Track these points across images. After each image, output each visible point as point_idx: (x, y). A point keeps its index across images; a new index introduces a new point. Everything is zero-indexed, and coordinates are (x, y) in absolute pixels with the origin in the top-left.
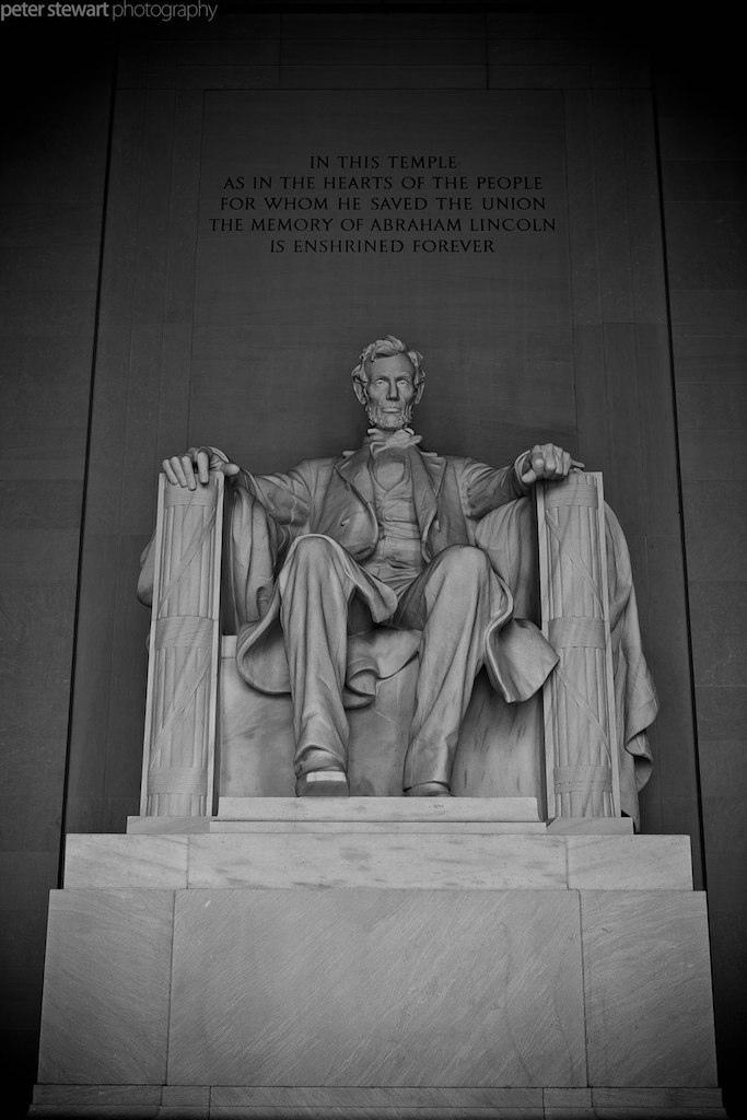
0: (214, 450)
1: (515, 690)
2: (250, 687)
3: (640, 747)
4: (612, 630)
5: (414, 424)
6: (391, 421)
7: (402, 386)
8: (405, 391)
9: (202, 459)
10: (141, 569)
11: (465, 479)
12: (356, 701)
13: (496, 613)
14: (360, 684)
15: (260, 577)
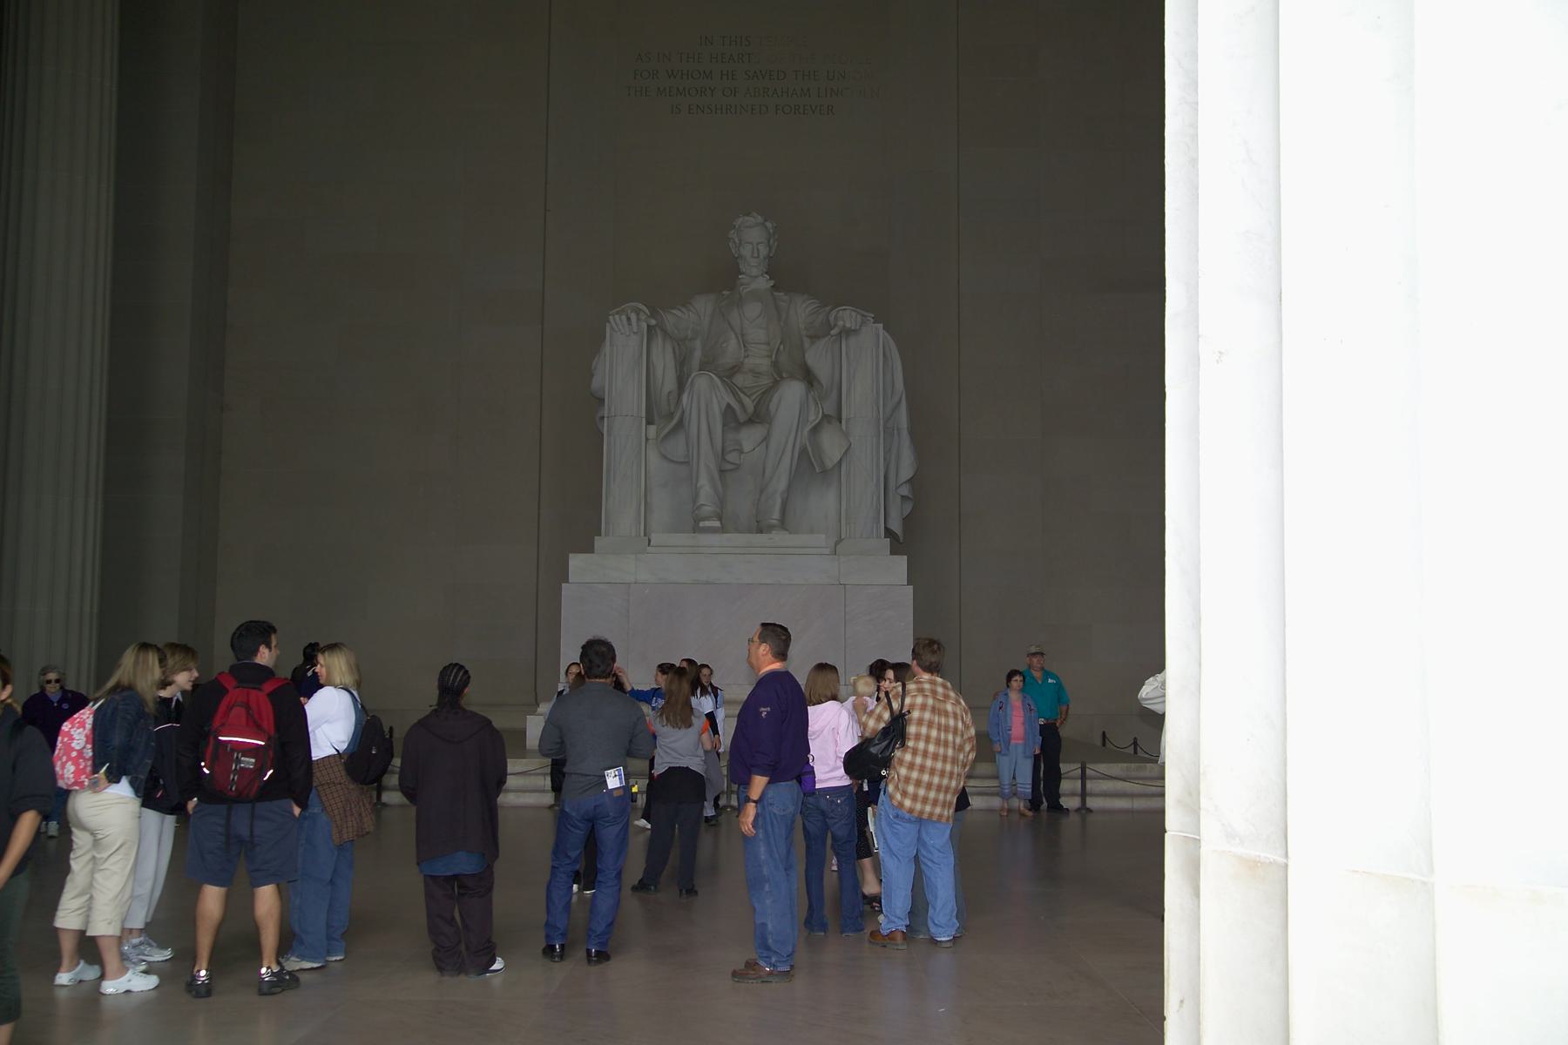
0: (641, 306)
1: (822, 463)
2: (665, 457)
3: (905, 491)
4: (887, 421)
5: (771, 272)
6: (755, 272)
7: (761, 247)
8: (764, 251)
9: (633, 317)
10: (592, 375)
11: (802, 310)
12: (729, 467)
13: (812, 418)
14: (732, 457)
15: (670, 384)
